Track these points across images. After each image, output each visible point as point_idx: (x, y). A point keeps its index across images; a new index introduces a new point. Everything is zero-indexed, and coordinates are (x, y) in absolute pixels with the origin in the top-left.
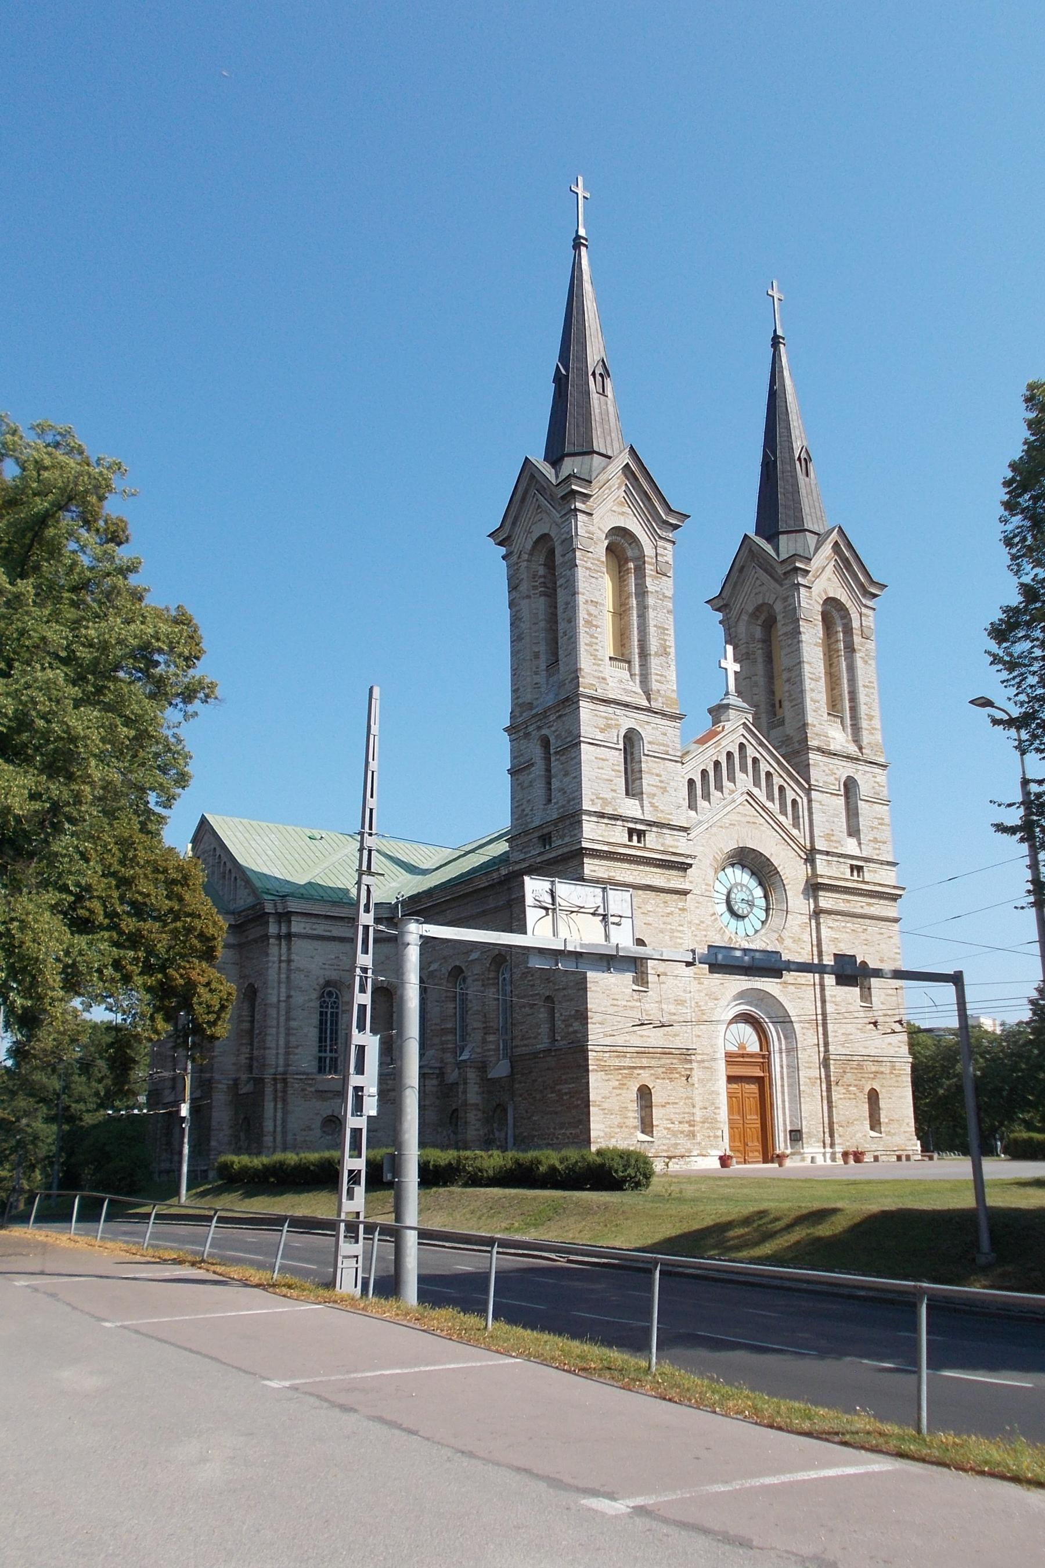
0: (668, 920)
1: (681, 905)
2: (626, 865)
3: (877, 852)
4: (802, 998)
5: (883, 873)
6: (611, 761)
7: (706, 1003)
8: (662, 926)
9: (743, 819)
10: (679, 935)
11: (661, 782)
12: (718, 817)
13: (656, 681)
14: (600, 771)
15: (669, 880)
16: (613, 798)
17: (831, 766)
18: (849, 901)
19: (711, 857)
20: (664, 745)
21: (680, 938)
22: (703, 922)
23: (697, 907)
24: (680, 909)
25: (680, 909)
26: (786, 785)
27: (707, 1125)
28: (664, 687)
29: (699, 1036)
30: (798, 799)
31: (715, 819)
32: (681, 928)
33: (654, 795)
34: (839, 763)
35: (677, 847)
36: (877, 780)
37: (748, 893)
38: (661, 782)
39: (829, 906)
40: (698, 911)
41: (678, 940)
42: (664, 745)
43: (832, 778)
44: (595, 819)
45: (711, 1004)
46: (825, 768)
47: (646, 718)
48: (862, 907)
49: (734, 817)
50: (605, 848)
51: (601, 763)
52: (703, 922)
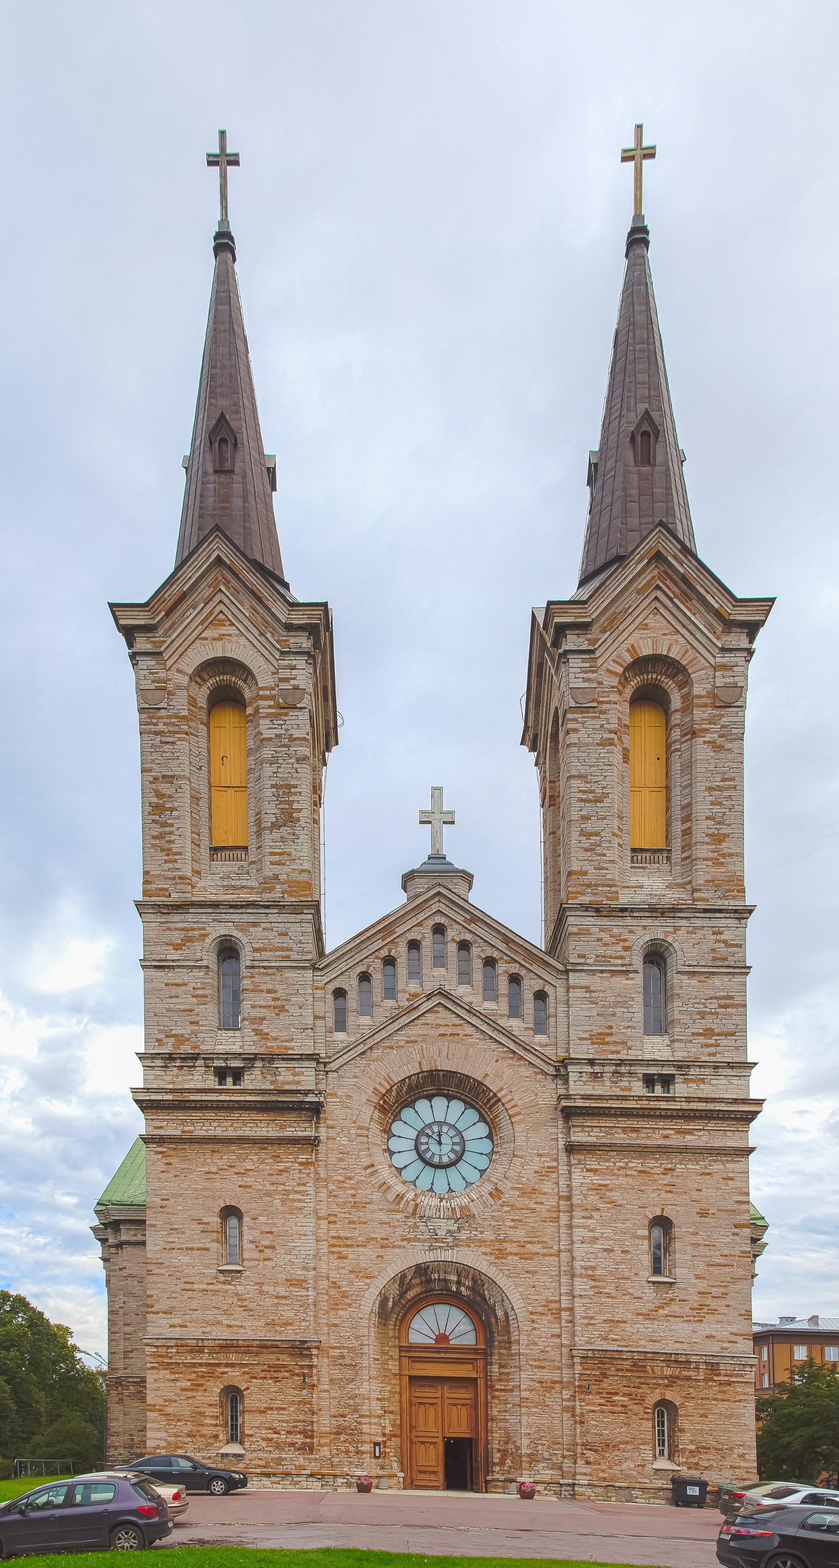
0: (280, 1179)
1: (302, 1158)
3: (712, 1050)
4: (534, 1273)
5: (723, 1081)
7: (351, 1283)
8: (269, 1188)
10: (298, 1196)
15: (282, 1127)
18: (636, 1130)
21: (300, 1201)
24: (301, 1164)
25: (301, 1164)
27: (343, 1437)
29: (336, 1325)
32: (303, 1188)
35: (298, 1083)
41: (296, 1204)
45: (360, 1284)
48: (666, 1137)
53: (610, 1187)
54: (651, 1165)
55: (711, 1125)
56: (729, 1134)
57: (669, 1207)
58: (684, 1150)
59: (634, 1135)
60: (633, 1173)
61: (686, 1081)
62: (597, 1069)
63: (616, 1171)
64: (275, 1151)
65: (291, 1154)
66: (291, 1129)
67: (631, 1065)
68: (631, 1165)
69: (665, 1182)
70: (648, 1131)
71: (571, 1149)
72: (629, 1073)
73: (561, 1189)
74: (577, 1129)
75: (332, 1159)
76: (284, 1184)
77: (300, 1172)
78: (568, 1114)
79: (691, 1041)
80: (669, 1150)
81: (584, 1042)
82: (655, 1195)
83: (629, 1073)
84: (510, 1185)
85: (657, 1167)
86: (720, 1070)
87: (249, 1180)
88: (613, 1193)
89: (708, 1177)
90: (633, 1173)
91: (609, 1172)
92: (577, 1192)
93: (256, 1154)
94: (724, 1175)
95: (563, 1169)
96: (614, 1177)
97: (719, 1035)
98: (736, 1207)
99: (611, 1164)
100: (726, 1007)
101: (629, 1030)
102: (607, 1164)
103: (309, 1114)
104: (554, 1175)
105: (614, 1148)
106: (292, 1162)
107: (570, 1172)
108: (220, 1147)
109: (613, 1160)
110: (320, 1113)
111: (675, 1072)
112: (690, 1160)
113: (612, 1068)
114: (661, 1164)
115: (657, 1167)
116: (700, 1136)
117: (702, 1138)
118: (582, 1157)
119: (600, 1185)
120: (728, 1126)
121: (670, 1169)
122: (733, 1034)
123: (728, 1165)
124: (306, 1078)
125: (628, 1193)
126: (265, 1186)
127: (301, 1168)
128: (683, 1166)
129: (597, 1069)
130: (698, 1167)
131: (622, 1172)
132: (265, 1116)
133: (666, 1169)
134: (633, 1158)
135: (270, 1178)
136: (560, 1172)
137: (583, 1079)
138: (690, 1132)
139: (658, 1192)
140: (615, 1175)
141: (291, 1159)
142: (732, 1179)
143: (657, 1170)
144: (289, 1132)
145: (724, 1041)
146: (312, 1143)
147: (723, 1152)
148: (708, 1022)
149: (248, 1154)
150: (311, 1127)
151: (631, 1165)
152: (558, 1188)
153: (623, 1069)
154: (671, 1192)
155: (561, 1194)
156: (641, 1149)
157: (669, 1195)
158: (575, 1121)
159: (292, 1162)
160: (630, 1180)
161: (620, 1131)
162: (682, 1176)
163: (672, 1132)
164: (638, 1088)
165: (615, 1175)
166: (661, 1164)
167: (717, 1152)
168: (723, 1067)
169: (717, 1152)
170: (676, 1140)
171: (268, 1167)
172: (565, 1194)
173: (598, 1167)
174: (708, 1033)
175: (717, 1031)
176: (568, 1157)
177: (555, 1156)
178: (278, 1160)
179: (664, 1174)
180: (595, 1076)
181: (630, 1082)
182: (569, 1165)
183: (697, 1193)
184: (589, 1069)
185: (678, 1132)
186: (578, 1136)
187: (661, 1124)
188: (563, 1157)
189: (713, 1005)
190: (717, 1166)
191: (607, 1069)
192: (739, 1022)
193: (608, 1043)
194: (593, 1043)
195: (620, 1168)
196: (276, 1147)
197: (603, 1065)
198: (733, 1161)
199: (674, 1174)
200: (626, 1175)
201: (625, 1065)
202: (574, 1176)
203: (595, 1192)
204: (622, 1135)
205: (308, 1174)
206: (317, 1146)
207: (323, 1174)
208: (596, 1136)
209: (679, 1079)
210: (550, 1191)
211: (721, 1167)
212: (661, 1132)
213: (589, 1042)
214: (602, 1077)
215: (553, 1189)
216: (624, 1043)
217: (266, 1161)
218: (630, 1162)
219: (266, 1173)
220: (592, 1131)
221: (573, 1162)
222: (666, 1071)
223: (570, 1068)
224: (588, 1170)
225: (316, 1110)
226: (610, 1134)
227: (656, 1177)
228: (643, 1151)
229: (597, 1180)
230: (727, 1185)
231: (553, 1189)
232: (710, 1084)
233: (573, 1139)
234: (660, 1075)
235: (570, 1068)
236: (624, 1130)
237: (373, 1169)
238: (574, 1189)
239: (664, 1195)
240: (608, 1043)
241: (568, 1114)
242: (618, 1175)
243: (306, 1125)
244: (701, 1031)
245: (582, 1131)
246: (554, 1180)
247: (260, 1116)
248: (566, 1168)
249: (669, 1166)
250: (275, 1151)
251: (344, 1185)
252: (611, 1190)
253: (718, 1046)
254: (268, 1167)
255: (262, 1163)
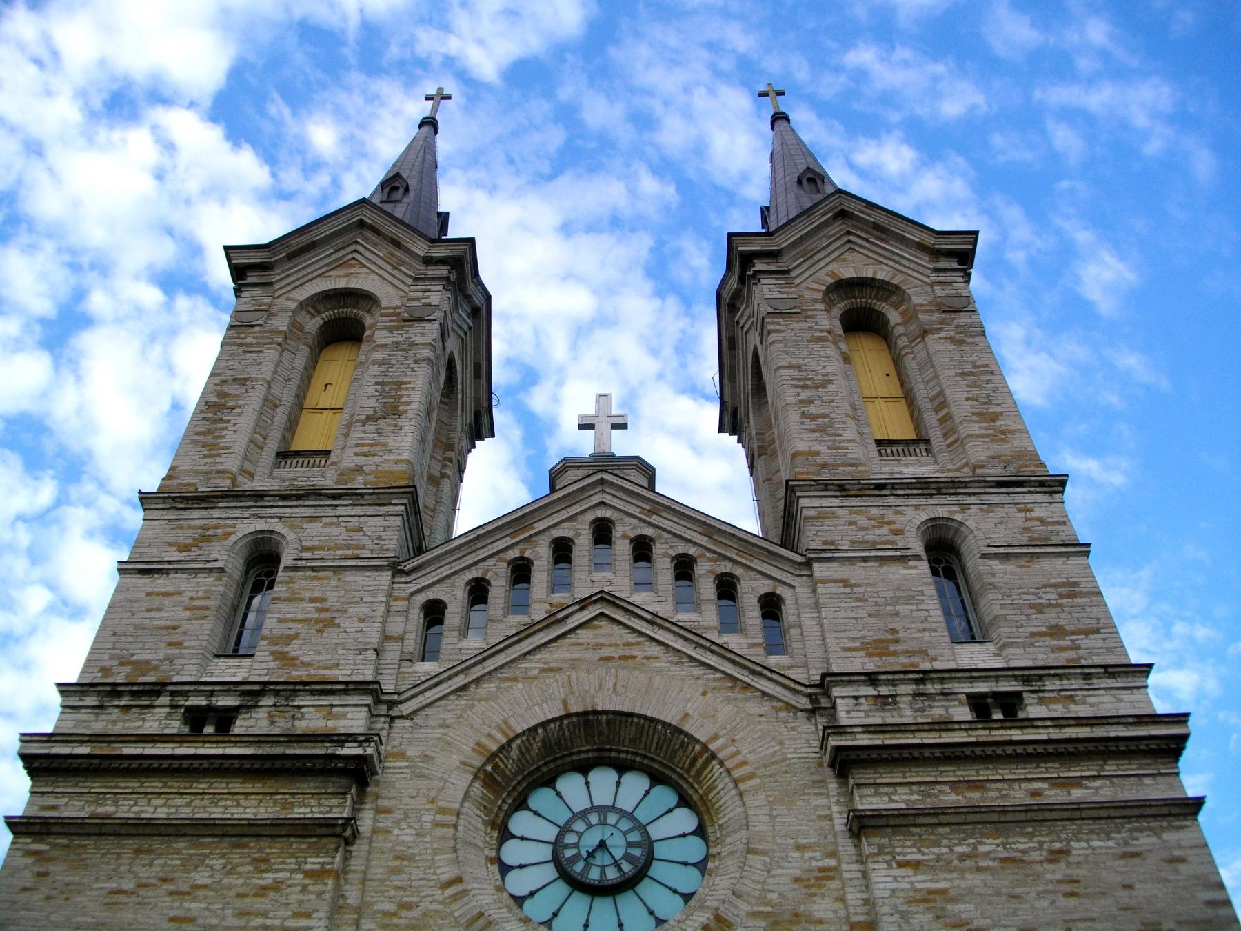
0: (259, 904)
1: (313, 863)
2: (154, 785)
6: (189, 594)
9: (589, 655)
11: (319, 610)
12: (501, 659)
13: (356, 454)
14: (153, 614)
16: (167, 658)
17: (874, 512)
19: (467, 747)
20: (348, 547)
22: (409, 906)
23: (396, 871)
24: (307, 874)
25: (307, 874)
26: (739, 572)
28: (376, 459)
30: (780, 590)
31: (490, 665)
33: (296, 637)
34: (898, 501)
36: (1034, 515)
37: (625, 825)
38: (319, 610)
39: (903, 806)
40: (397, 880)
42: (348, 547)
43: (884, 531)
44: (91, 701)
46: (855, 518)
47: (309, 512)
48: (1035, 794)
49: (557, 654)
50: (84, 750)
51: (156, 602)
52: (409, 906)
53: (952, 892)
54: (1021, 847)
55: (1111, 768)
56: (1147, 781)
57: (1079, 924)
58: (1077, 813)
59: (976, 795)
60: (991, 863)
61: (1042, 702)
62: (884, 690)
63: (956, 862)
64: (261, 850)
65: (292, 856)
66: (302, 810)
67: (942, 680)
68: (983, 849)
69: (1058, 876)
70: (1000, 785)
71: (861, 825)
72: (943, 694)
73: (851, 910)
74: (867, 791)
75: (377, 870)
76: (264, 915)
77: (304, 889)
78: (845, 763)
79: (1032, 645)
80: (1048, 815)
81: (854, 654)
82: (1044, 903)
83: (943, 694)
84: (744, 907)
85: (1034, 849)
86: (1095, 681)
87: (194, 906)
88: (961, 907)
89: (1136, 861)
90: (991, 863)
91: (943, 865)
92: (886, 909)
93: (223, 856)
94: (1165, 854)
95: (850, 870)
96: (955, 875)
97: (1073, 633)
98: (1210, 912)
99: (944, 850)
100: (1071, 596)
101: (927, 634)
102: (936, 850)
103: (344, 781)
104: (834, 884)
105: (944, 819)
106: (292, 871)
107: (865, 875)
108: (155, 843)
109: (945, 842)
110: (367, 785)
111: (1020, 688)
112: (1091, 832)
113: (910, 688)
114: (1041, 844)
115: (1034, 849)
116: (1097, 789)
117: (1101, 792)
118: (885, 841)
119: (930, 892)
120: (1141, 767)
121: (1061, 852)
122: (1097, 631)
123: (1166, 836)
124: (353, 717)
125: (990, 903)
126: (224, 918)
127: (307, 881)
128: (1084, 844)
129: (884, 690)
130: (1111, 843)
131: (968, 863)
132: (258, 787)
133: (1052, 852)
134: (982, 835)
135: (239, 903)
136: (846, 875)
137: (863, 708)
138: (1078, 782)
139: (1050, 897)
140: (956, 869)
141: (288, 866)
142: (1182, 860)
143: (1035, 856)
144: (300, 812)
145: (1085, 642)
146: (341, 834)
147: (1149, 811)
148: (1052, 617)
149: (206, 856)
150: (340, 805)
151: (983, 849)
152: (846, 907)
153: (930, 688)
154: (1072, 894)
155: (855, 919)
156: (995, 817)
157: (1073, 901)
158: (861, 776)
159: (292, 871)
160: (989, 877)
161: (947, 789)
162: (1086, 862)
163: (1044, 785)
164: (963, 713)
165: (956, 869)
166: (1041, 844)
167: (1136, 812)
168: (1099, 676)
169: (1136, 812)
170: (1055, 796)
171: (241, 881)
172: (862, 918)
173: (919, 857)
174: (1056, 631)
175: (1069, 628)
176: (858, 846)
177: (831, 848)
178: (263, 866)
179: (1051, 861)
180: (882, 702)
181: (946, 708)
182: (861, 859)
183: (1126, 893)
184: (870, 691)
185: (1055, 782)
186: (868, 802)
187: (1020, 772)
188: (846, 846)
189: (1051, 595)
190: (1145, 841)
191: (902, 689)
192: (1100, 615)
193: (895, 654)
194: (869, 655)
195: (963, 857)
196: (264, 843)
197: (893, 683)
198: (1170, 828)
199: (1071, 859)
200: (979, 869)
201: (932, 680)
202: (875, 877)
203: (922, 906)
204: (953, 797)
205: (320, 894)
206: (348, 842)
207: (352, 896)
208: (905, 802)
209: (1029, 699)
210: (830, 915)
211: (1154, 839)
212: (1024, 785)
213: (862, 653)
214: (895, 703)
215: (835, 912)
216: (923, 652)
217: (241, 869)
218: (981, 843)
219: (233, 893)
220: (896, 793)
221: (867, 850)
222: (1004, 687)
223: (836, 692)
224: (901, 865)
225: (358, 774)
226: (930, 795)
227: (1038, 868)
228: (1000, 820)
229: (923, 881)
230: (1177, 872)
231: (835, 912)
232: (1085, 703)
233: (860, 807)
234: (996, 695)
235: (836, 692)
236: (955, 785)
237: (460, 887)
238: (880, 902)
239: (1062, 902)
240: (895, 654)
241: (845, 763)
242: (963, 871)
243: (334, 801)
244: (1044, 629)
245: (876, 794)
246: (836, 894)
247: (248, 788)
248: (855, 867)
249: (1058, 845)
250: (261, 850)
251: (395, 921)
252: (955, 900)
253: (1079, 648)
254: (241, 881)
255: (229, 873)
